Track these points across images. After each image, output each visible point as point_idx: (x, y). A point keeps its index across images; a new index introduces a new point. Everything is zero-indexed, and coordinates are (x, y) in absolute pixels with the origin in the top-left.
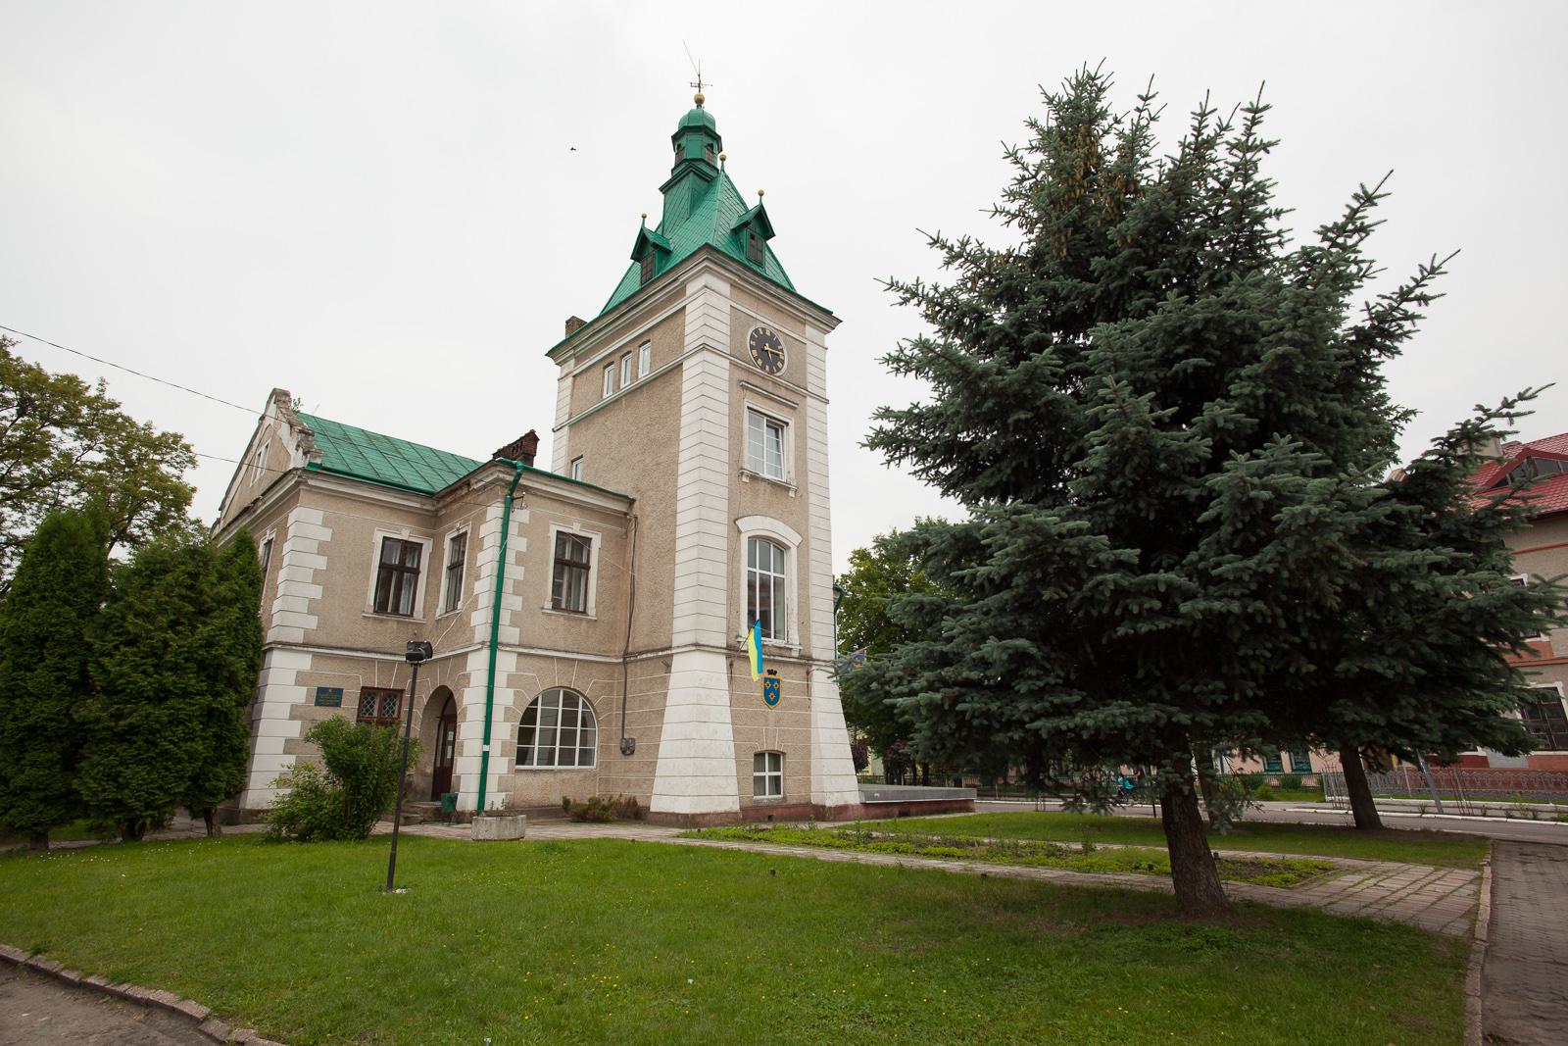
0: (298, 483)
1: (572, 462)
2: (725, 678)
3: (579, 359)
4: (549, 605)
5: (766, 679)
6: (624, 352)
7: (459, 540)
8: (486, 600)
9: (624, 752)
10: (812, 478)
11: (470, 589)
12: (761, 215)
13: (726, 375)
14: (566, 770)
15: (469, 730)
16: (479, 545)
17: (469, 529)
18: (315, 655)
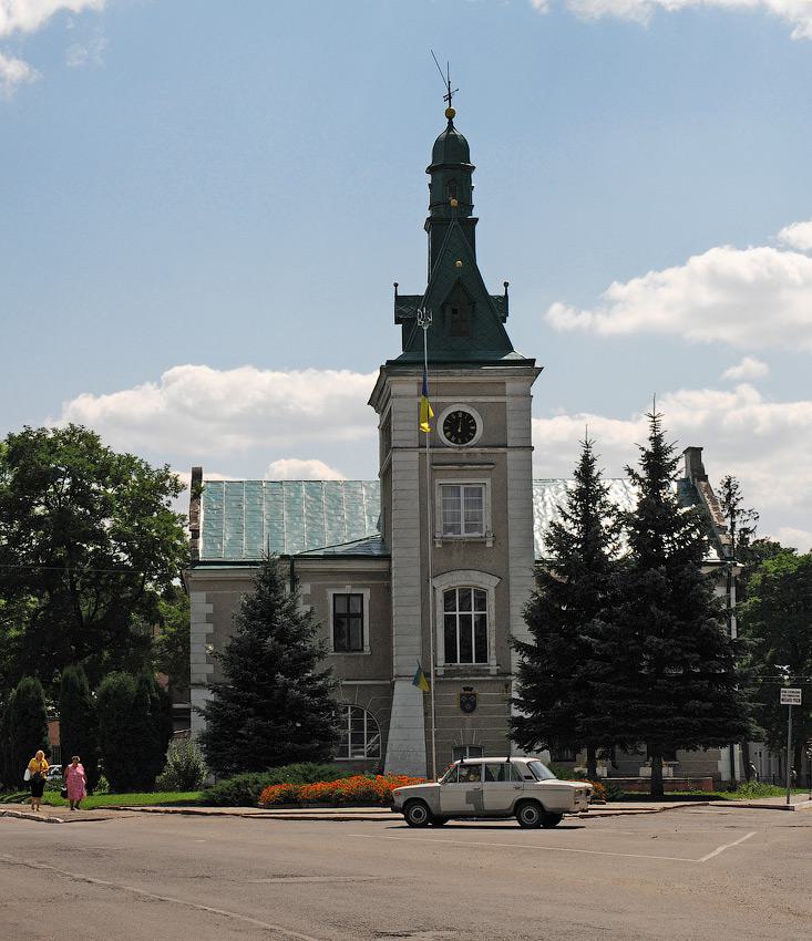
5: (462, 695)
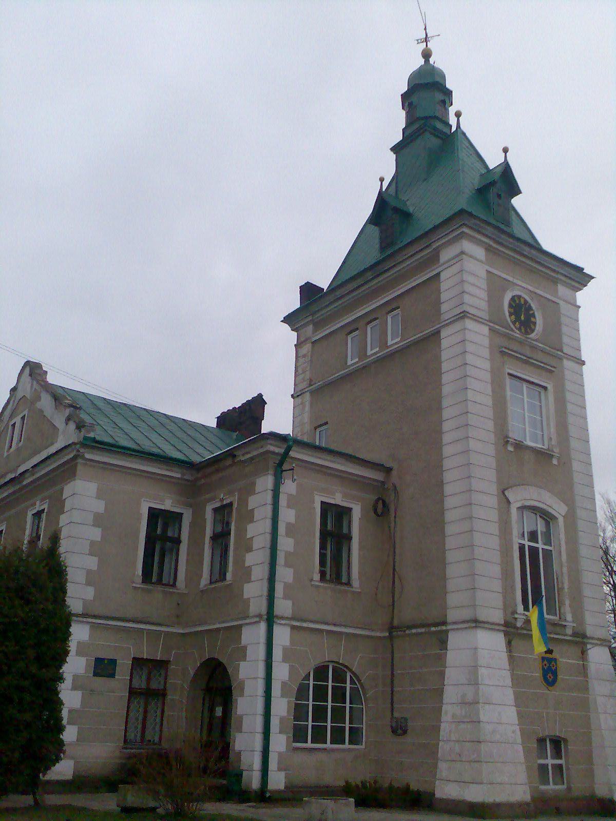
0: (75, 458)
1: (315, 428)
2: (504, 656)
3: (318, 325)
4: (317, 577)
6: (369, 318)
7: (224, 511)
8: (260, 572)
9: (394, 731)
10: (574, 444)
11: (240, 562)
12: (506, 171)
13: (486, 342)
14: (338, 750)
15: (248, 706)
16: (249, 516)
17: (235, 499)
18: (94, 627)
